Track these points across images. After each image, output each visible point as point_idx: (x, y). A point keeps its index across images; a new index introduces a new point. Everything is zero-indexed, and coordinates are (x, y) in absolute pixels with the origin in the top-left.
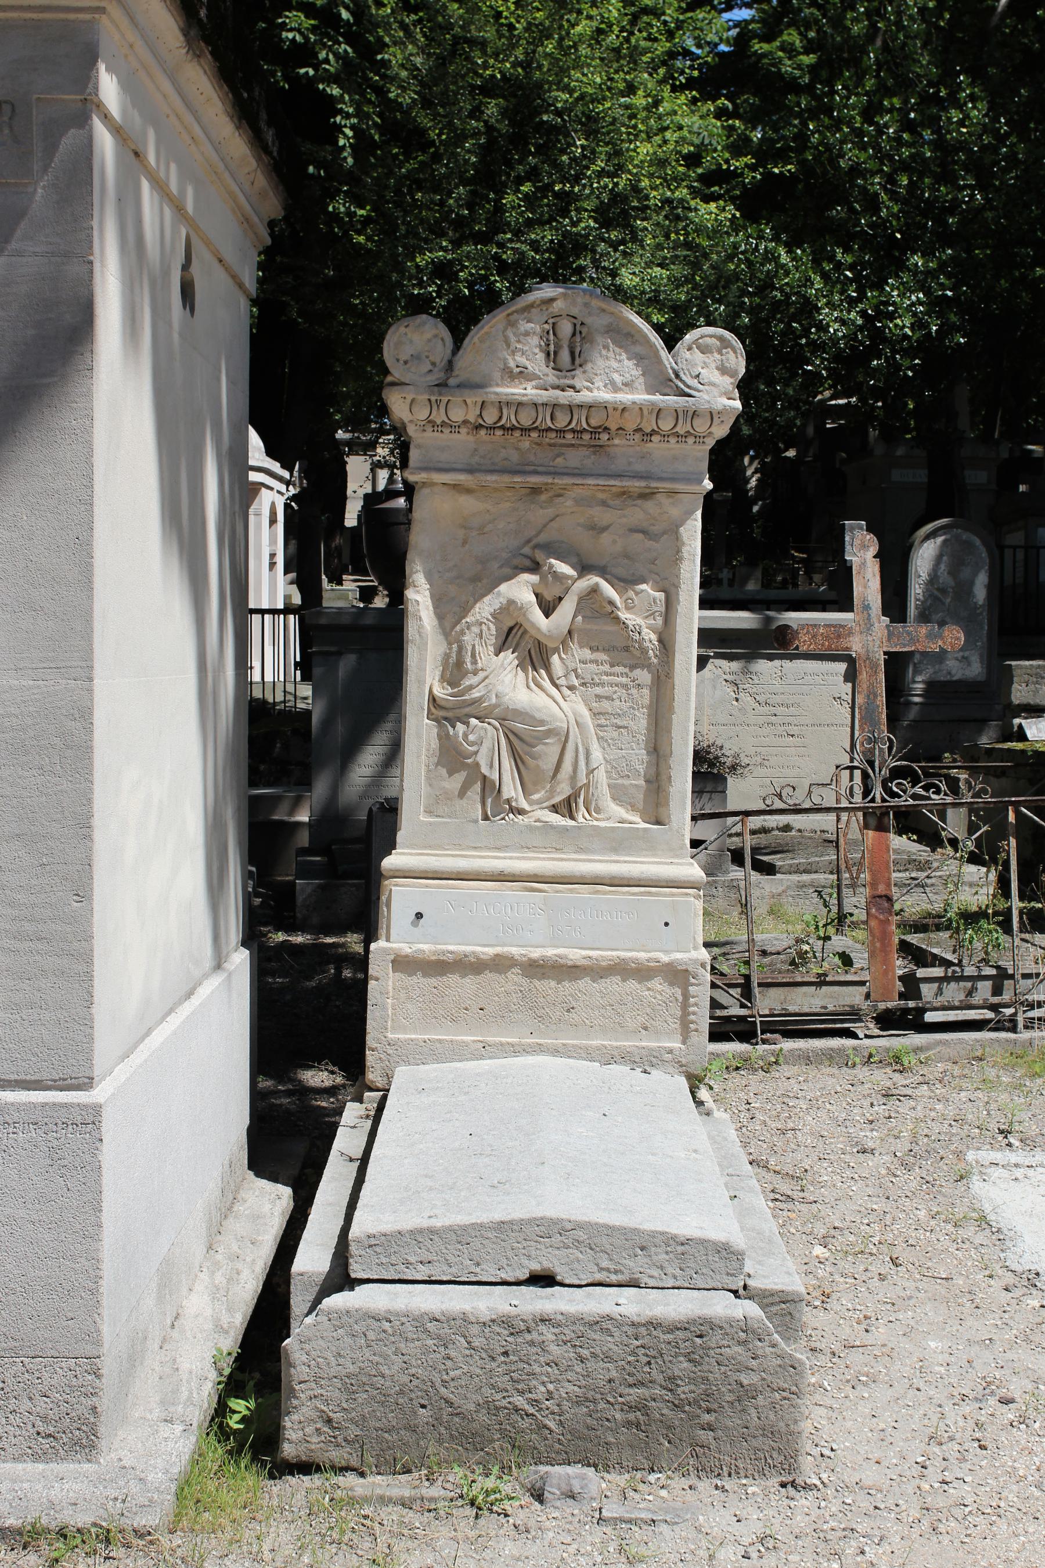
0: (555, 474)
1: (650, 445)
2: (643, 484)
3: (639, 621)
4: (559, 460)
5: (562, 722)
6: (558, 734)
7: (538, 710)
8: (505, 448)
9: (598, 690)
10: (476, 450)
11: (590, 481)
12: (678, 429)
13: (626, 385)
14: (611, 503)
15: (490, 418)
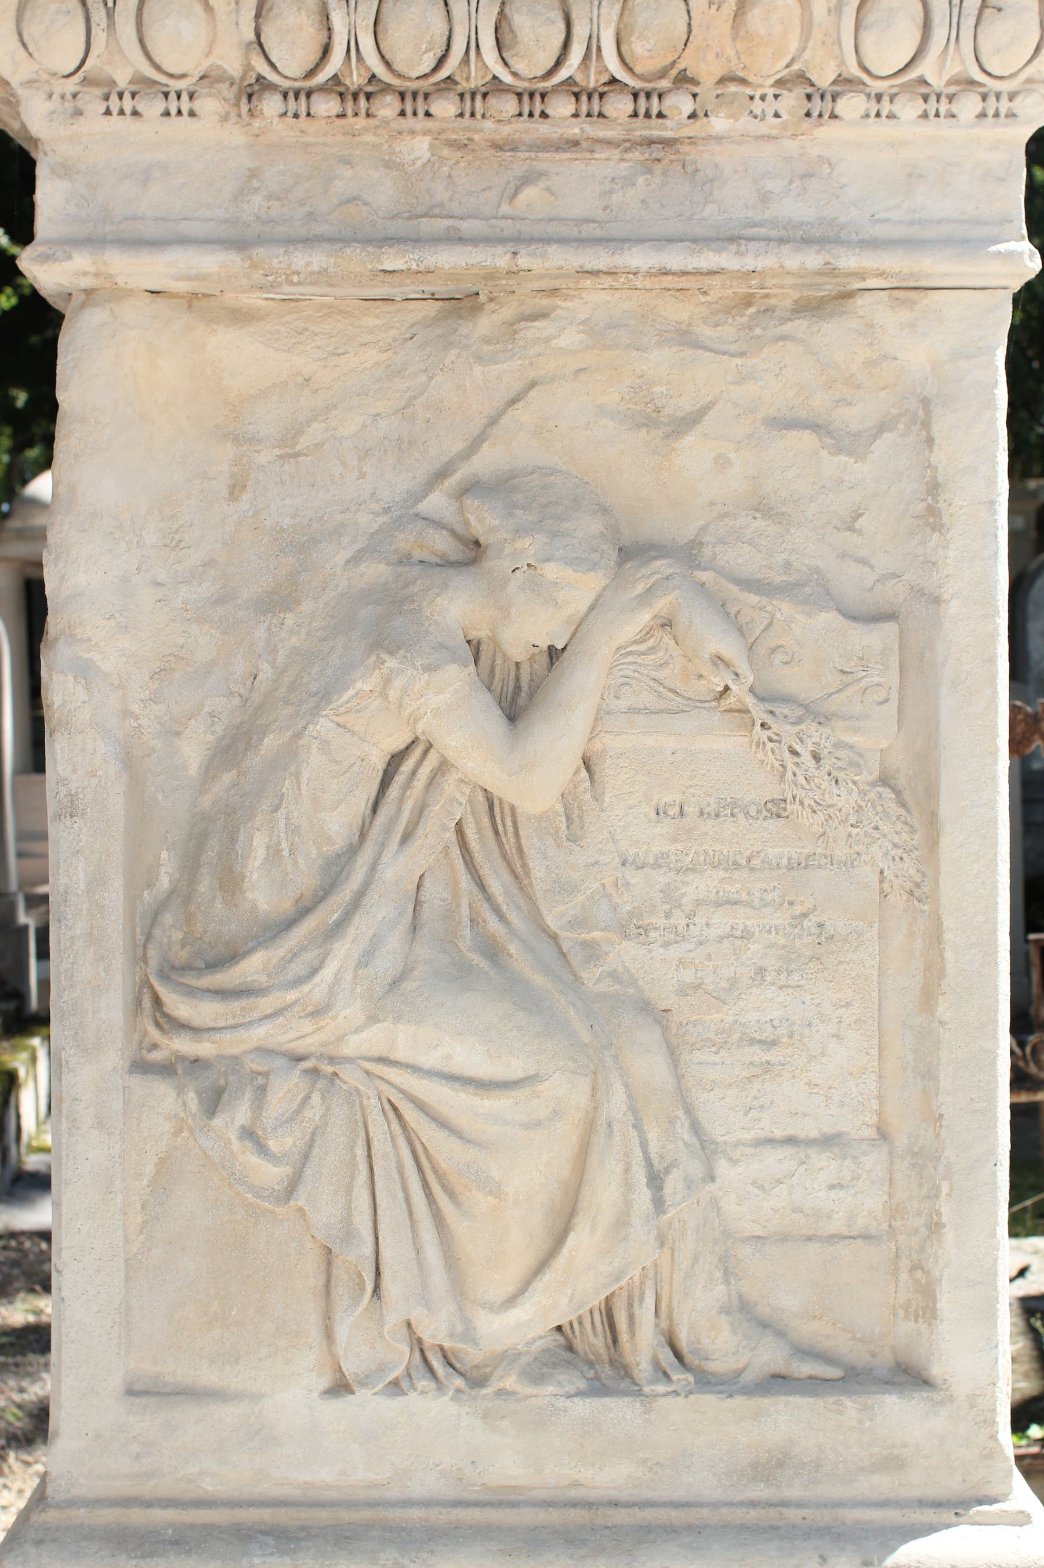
0: (518, 241)
1: (828, 132)
2: (813, 260)
4: (530, 194)
8: (348, 162)
10: (253, 174)
11: (637, 259)
12: (926, 69)
14: (705, 332)
15: (291, 54)
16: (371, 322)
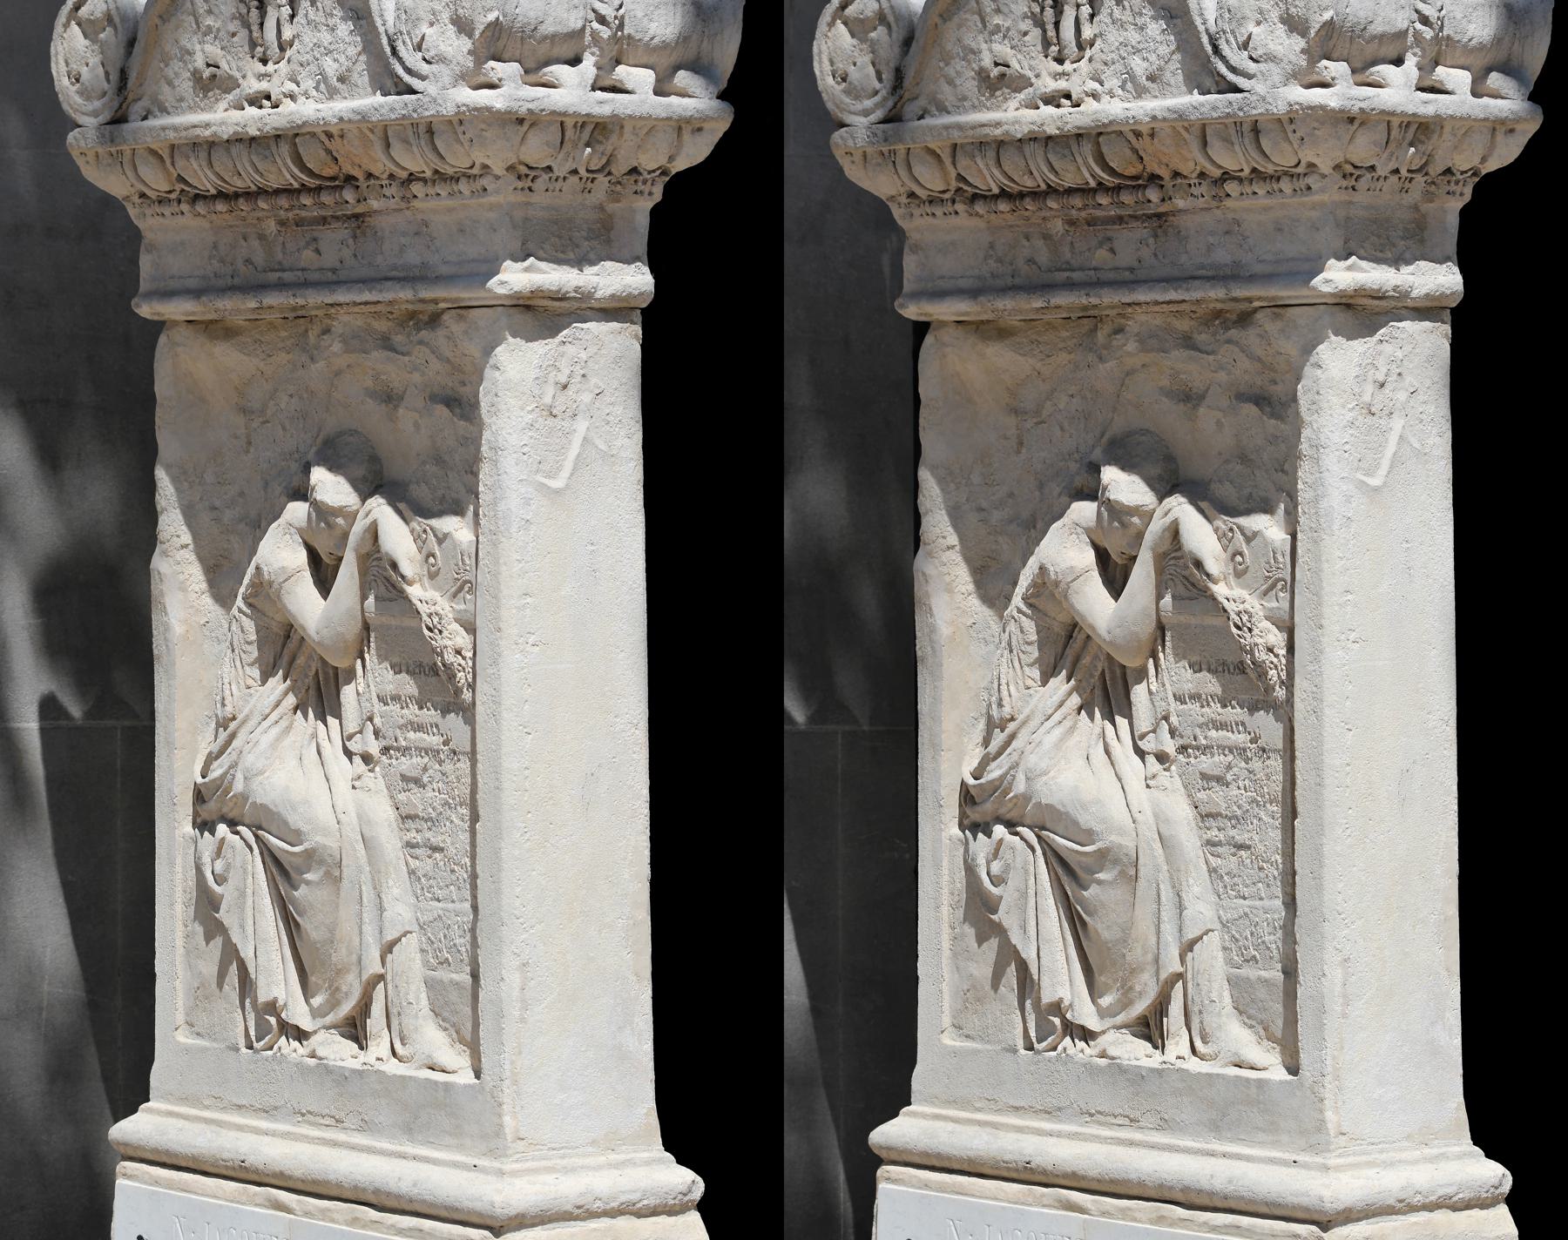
3: (1253, 604)
5: (1121, 831)
6: (1116, 862)
7: (1084, 807)
9: (1206, 763)
13: (1152, 78)
14: (1202, 338)
16: (1065, 334)
